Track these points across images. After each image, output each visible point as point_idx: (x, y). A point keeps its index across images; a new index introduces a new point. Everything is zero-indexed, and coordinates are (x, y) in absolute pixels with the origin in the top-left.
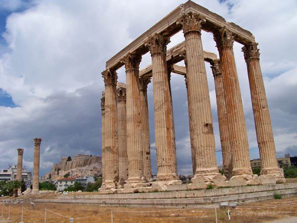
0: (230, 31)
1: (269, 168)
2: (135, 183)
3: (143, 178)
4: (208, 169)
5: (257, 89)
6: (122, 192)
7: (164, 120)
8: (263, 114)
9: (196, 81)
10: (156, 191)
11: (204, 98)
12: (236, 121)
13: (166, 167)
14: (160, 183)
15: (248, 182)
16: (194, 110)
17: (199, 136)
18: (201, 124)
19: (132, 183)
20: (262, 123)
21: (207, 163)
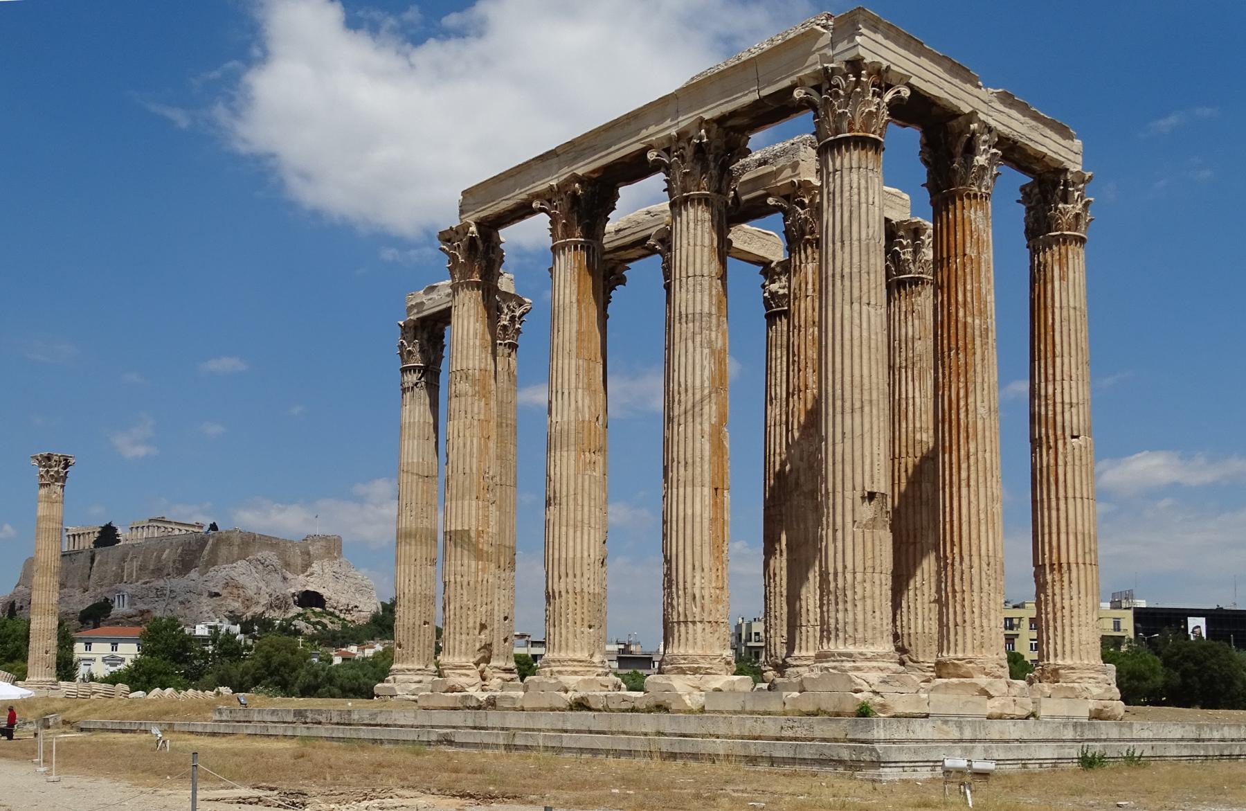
1: (1068, 662)
2: (576, 673)
4: (863, 649)
8: (1069, 459)
12: (969, 486)
14: (680, 683)
15: (992, 706)
19: (560, 672)
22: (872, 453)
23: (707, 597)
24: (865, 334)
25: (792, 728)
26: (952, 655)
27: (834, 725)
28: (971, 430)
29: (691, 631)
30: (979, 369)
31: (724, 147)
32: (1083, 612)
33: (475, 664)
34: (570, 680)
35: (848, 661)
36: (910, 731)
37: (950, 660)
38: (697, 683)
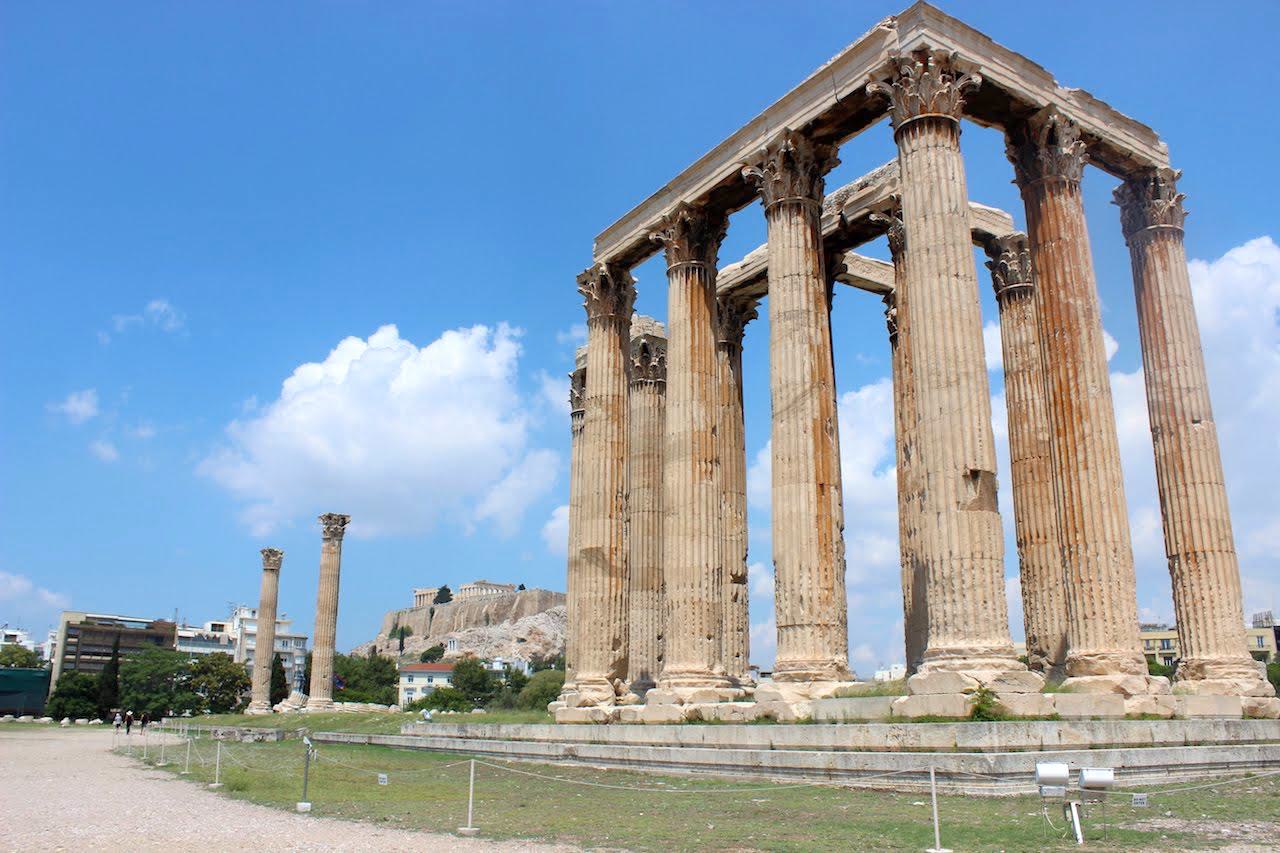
0: (1071, 124)
1: (1214, 656)
3: (717, 670)
4: (975, 644)
5: (1170, 348)
6: (638, 719)
7: (806, 454)
8: (1193, 444)
9: (937, 308)
10: (768, 719)
11: (967, 374)
12: (1086, 468)
13: (808, 630)
15: (1131, 706)
16: (927, 418)
17: (943, 517)
18: (951, 473)
19: (677, 684)
20: (1189, 480)
21: (971, 622)
22: (972, 428)
23: (815, 598)
24: (955, 305)
25: (897, 737)
26: (1083, 651)
27: (942, 732)
28: (1083, 411)
29: (799, 635)
30: (1086, 347)
31: (813, 157)
32: (1224, 602)
33: (609, 679)
34: (687, 692)
35: (958, 658)
36: (1031, 737)
37: (1081, 656)
38: (807, 691)
